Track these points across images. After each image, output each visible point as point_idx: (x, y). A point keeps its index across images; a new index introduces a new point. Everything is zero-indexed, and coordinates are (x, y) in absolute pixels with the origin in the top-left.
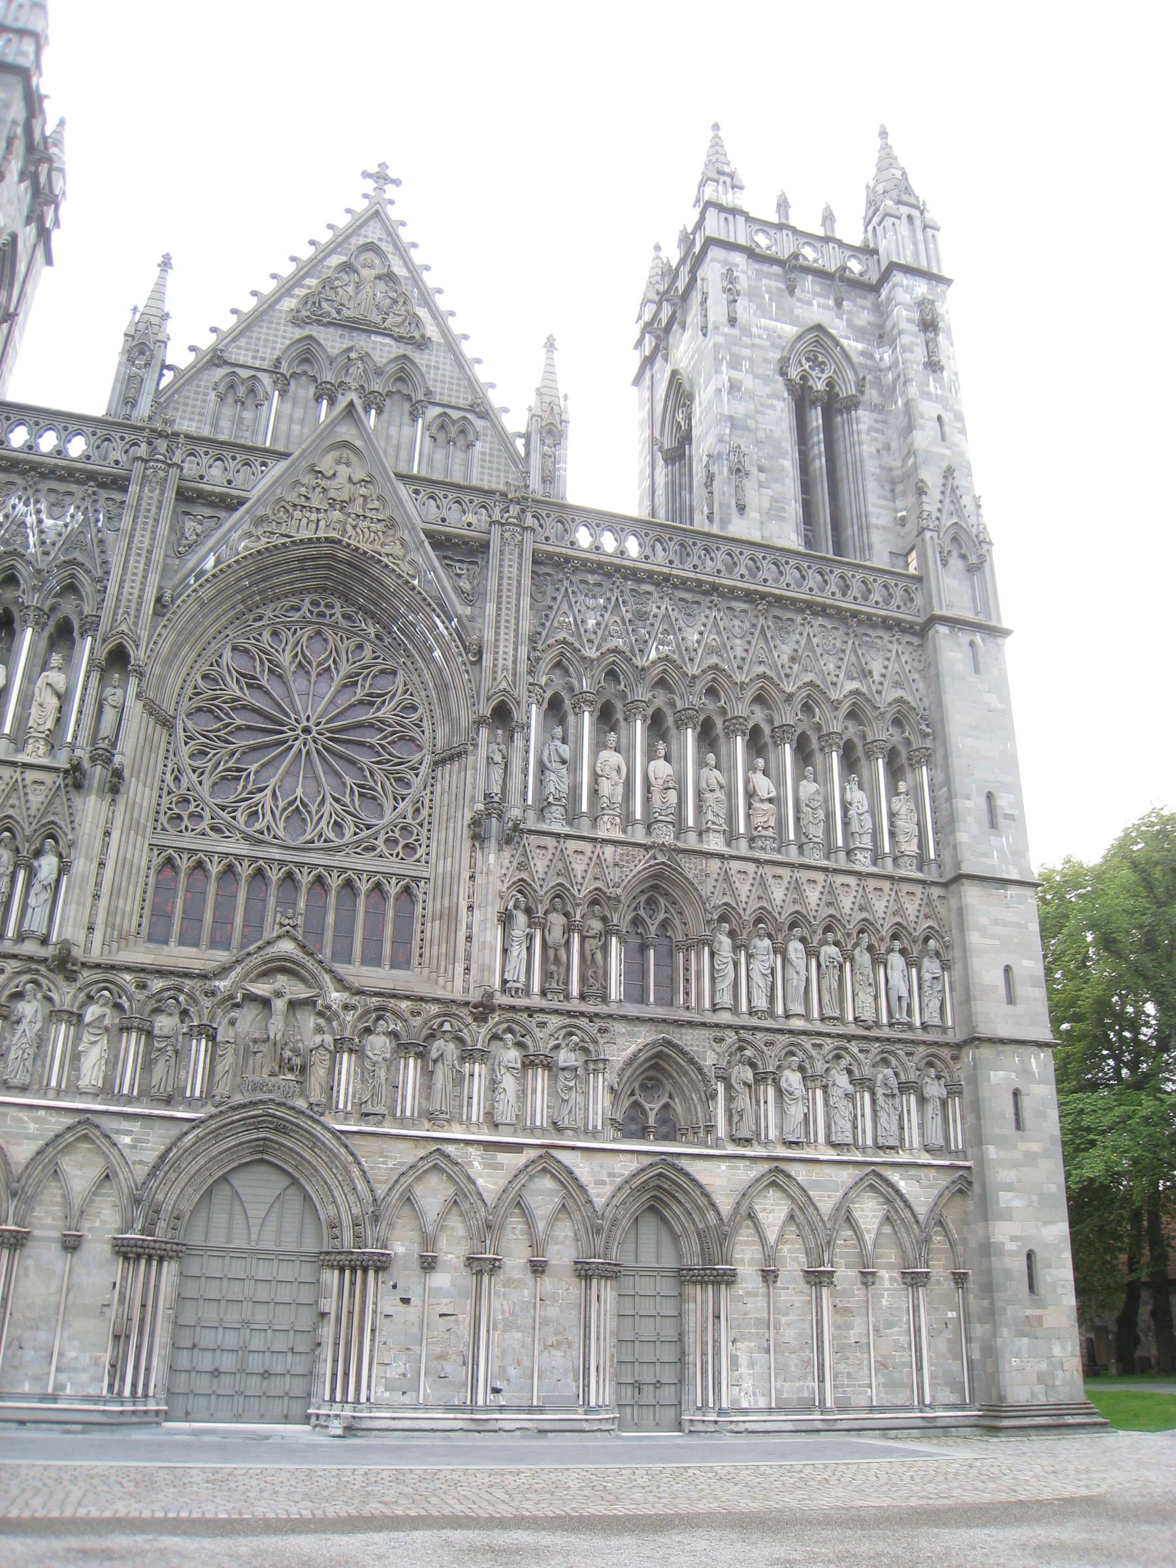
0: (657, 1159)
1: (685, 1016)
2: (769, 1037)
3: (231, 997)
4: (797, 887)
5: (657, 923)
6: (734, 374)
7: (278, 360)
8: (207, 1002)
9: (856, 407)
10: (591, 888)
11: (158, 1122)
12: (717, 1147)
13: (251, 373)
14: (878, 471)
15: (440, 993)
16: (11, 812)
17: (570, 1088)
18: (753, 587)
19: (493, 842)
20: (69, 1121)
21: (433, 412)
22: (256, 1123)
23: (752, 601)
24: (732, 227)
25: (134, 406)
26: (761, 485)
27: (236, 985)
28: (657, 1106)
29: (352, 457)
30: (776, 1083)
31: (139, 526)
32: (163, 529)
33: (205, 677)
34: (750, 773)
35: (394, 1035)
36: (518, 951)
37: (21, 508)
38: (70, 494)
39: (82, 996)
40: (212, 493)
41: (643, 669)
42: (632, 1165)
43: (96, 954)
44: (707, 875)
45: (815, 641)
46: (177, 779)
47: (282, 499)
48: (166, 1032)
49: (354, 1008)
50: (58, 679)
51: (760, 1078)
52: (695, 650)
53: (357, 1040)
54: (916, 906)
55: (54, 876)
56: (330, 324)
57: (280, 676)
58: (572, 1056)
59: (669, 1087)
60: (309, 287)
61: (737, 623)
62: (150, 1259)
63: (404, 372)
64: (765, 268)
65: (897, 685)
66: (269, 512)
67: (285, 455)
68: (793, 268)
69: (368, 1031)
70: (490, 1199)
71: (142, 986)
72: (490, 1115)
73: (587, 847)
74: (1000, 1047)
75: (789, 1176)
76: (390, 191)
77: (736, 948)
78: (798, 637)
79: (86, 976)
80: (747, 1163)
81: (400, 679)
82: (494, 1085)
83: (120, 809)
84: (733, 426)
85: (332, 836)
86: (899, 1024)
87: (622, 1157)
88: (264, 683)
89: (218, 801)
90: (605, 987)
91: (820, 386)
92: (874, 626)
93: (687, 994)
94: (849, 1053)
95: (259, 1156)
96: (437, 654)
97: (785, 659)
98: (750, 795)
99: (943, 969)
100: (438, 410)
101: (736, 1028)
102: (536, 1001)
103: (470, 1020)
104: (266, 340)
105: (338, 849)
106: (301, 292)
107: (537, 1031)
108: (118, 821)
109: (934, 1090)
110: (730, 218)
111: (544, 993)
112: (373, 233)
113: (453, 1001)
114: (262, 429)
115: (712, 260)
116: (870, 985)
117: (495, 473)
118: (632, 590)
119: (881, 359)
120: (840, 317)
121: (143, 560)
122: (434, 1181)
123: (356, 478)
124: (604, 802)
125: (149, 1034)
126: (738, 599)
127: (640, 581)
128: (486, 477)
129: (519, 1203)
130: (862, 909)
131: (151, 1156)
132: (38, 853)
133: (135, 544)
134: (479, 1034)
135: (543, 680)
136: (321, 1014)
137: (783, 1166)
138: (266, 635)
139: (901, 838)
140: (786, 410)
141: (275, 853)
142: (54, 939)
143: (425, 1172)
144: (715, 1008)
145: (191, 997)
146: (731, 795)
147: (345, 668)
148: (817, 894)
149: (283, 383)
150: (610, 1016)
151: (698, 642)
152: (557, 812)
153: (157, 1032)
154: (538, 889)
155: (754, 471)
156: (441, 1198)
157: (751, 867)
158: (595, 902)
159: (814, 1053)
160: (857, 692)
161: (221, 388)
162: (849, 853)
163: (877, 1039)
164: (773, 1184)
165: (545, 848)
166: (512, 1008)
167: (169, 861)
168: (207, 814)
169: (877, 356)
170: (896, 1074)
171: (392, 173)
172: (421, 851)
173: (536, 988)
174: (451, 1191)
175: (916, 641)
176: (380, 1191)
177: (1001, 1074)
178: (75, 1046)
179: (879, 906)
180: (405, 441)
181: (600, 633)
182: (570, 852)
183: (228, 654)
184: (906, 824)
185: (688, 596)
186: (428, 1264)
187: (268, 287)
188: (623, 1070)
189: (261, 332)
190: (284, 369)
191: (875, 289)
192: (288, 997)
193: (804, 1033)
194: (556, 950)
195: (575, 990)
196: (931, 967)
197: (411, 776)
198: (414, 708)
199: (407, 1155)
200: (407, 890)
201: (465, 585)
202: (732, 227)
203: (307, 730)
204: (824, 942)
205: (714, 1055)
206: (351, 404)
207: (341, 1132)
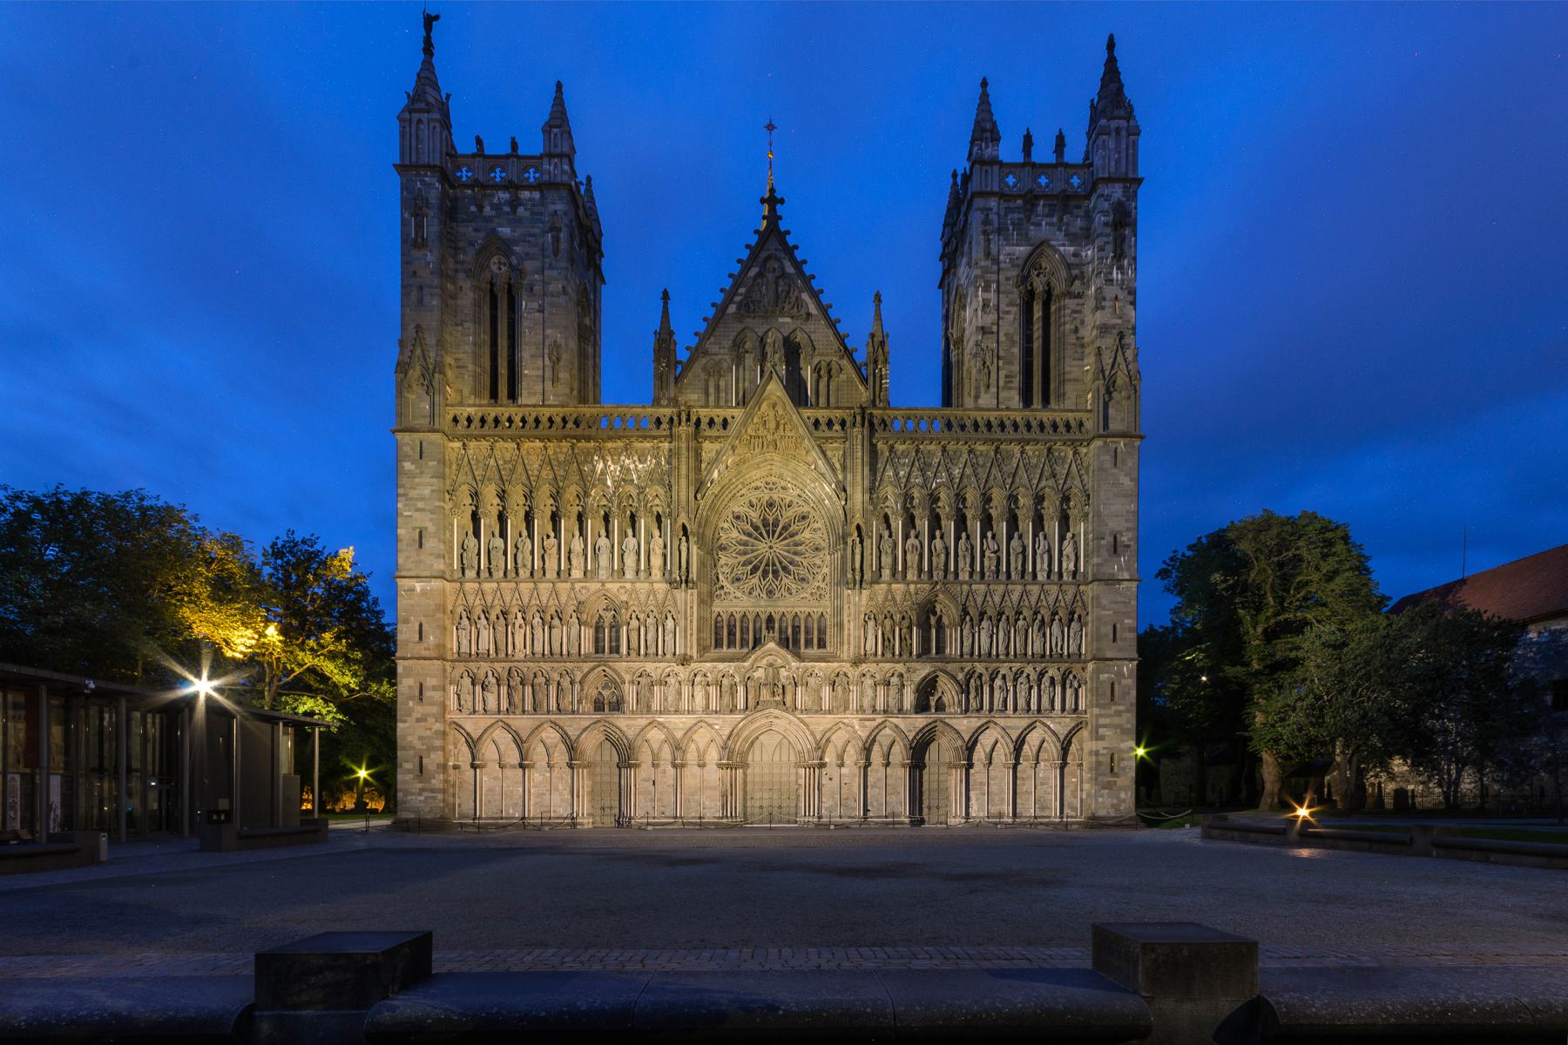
6: (987, 295)
14: (1074, 341)
24: (990, 178)
36: (871, 637)
37: (627, 461)
60: (741, 295)
64: (1011, 205)
68: (1031, 199)
84: (984, 333)
93: (951, 648)
96: (827, 502)
106: (737, 299)
110: (989, 169)
111: (883, 655)
115: (977, 209)
119: (1086, 256)
120: (1060, 229)
124: (909, 564)
131: (727, 732)
142: (677, 653)
173: (880, 652)
176: (818, 737)
177: (1106, 675)
186: (841, 765)
188: (919, 684)
191: (1088, 197)
195: (897, 653)
202: (990, 178)
203: (771, 548)
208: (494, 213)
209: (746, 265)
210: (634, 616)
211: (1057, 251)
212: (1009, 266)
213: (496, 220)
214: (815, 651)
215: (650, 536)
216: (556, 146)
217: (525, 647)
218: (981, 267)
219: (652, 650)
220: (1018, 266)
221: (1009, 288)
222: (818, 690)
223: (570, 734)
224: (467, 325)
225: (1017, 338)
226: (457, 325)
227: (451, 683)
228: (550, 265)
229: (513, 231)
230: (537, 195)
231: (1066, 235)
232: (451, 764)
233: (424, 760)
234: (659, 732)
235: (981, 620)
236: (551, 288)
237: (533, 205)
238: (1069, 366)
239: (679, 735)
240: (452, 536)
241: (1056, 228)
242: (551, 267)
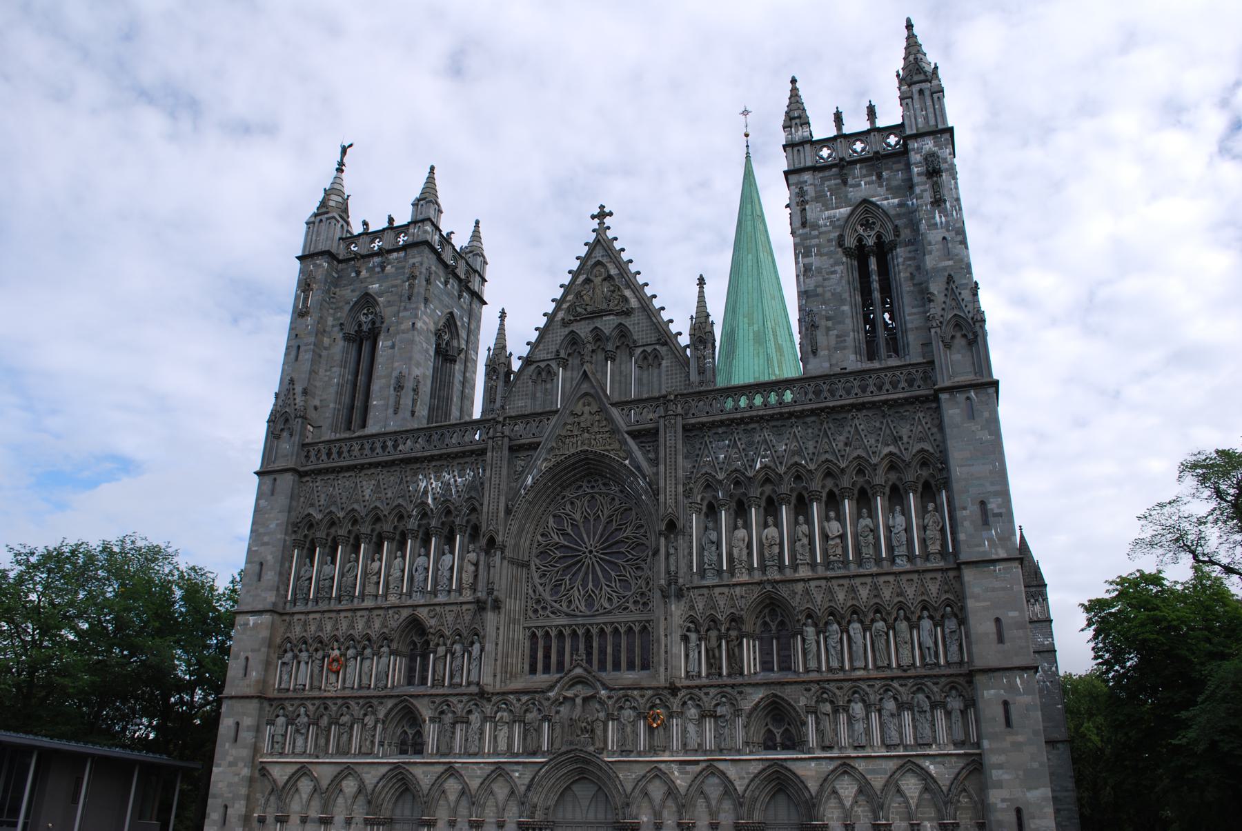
0: (772, 763)
1: (790, 677)
2: (839, 684)
3: (557, 700)
4: (853, 589)
5: (776, 622)
6: (807, 260)
7: (558, 351)
8: (546, 704)
9: (895, 248)
10: (728, 613)
11: (529, 765)
12: (809, 753)
13: (545, 363)
14: (912, 288)
15: (654, 684)
16: (458, 627)
17: (724, 727)
18: (814, 406)
19: (673, 598)
20: (492, 768)
21: (639, 351)
22: (577, 759)
23: (818, 415)
24: (802, 155)
25: (494, 402)
26: (828, 329)
27: (559, 694)
28: (781, 731)
29: (591, 399)
30: (846, 709)
31: (493, 473)
32: (504, 471)
33: (542, 535)
34: (826, 524)
35: (634, 708)
36: (694, 655)
38: (467, 463)
39: (495, 708)
40: (524, 444)
41: (750, 478)
42: (760, 766)
43: (499, 687)
44: (796, 593)
45: (860, 428)
46: (534, 591)
47: (559, 435)
48: (530, 721)
49: (613, 697)
50: (472, 556)
51: (836, 711)
52: (783, 456)
53: (616, 713)
54: (937, 587)
55: (479, 653)
56: (581, 319)
57: (577, 526)
58: (724, 708)
59: (787, 719)
60: (570, 301)
61: (810, 431)
63: (623, 332)
64: (827, 173)
65: (921, 440)
66: (555, 445)
67: (557, 411)
69: (621, 708)
70: (683, 791)
71: (519, 700)
72: (685, 745)
73: (726, 590)
74: (991, 674)
75: (853, 767)
76: (608, 221)
77: (818, 634)
78: (849, 428)
79: (494, 699)
80: (828, 761)
81: (633, 512)
82: (685, 731)
83: (502, 616)
84: (807, 297)
85: (606, 605)
86: (927, 664)
87: (753, 763)
88: (569, 531)
89: (553, 599)
90: (742, 668)
91: (870, 242)
92: (902, 405)
94: (893, 688)
95: (581, 776)
97: (841, 445)
98: (825, 537)
99: (960, 625)
100: (641, 349)
101: (818, 682)
102: (704, 681)
103: (669, 696)
104: (552, 341)
105: (610, 612)
106: (565, 306)
107: (705, 698)
108: (502, 622)
109: (955, 704)
110: (801, 148)
111: (708, 676)
112: (598, 254)
113: (658, 688)
114: (555, 392)
116: (906, 643)
117: (674, 377)
118: (744, 430)
119: (913, 204)
120: (881, 186)
121: (497, 490)
122: (657, 782)
123: (593, 411)
125: (524, 721)
126: (808, 416)
127: (748, 423)
128: (670, 381)
129: (702, 792)
130: (898, 595)
131: (527, 781)
132: (472, 643)
133: (493, 483)
134: (675, 704)
135: (699, 497)
136: (599, 702)
137: (847, 761)
138: (568, 506)
139: (929, 543)
140: (845, 271)
141: (580, 621)
143: (653, 777)
144: (807, 671)
145: (539, 701)
146: (811, 537)
147: (606, 513)
148: (867, 591)
149: (564, 364)
150: (742, 684)
151: (785, 450)
152: (709, 574)
153: (526, 721)
154: (699, 619)
155: (823, 323)
156: (662, 792)
157: (823, 583)
158: (733, 620)
159: (868, 689)
160: (891, 454)
161: (534, 377)
162: (892, 559)
163: (910, 677)
164: (845, 772)
165: (703, 595)
166: (688, 687)
167: (534, 635)
168: (549, 607)
169: (910, 203)
170: (928, 697)
171: (607, 210)
172: (651, 605)
174: (666, 788)
175: (934, 405)
176: (629, 791)
178: (495, 731)
179: (910, 591)
180: (628, 372)
181: (726, 462)
182: (716, 594)
183: (551, 520)
184: (933, 533)
185: (779, 423)
187: (550, 307)
189: (549, 337)
190: (562, 355)
192: (581, 697)
193: (860, 679)
194: (713, 651)
196: (951, 624)
197: (643, 565)
198: (642, 526)
199: (640, 771)
200: (645, 628)
201: (652, 456)
203: (591, 552)
204: (873, 621)
205: (805, 699)
206: (585, 371)
207: (610, 762)
208: (368, 275)
209: (575, 274)
210: (441, 643)
211: (878, 207)
212: (831, 228)
213: (369, 280)
214: (629, 677)
215: (465, 550)
216: (421, 214)
217: (337, 682)
218: (800, 235)
219: (457, 680)
220: (839, 226)
221: (832, 248)
222: (634, 724)
223: (367, 782)
224: (334, 369)
225: (846, 295)
226: (326, 371)
227: (267, 724)
228: (405, 307)
229: (380, 286)
230: (402, 254)
231: (887, 190)
232: (255, 815)
233: (230, 811)
234: (456, 781)
235: (827, 623)
236: (403, 327)
237: (398, 262)
238: (909, 315)
239: (474, 784)
240: (290, 568)
241: (877, 185)
242: (405, 309)
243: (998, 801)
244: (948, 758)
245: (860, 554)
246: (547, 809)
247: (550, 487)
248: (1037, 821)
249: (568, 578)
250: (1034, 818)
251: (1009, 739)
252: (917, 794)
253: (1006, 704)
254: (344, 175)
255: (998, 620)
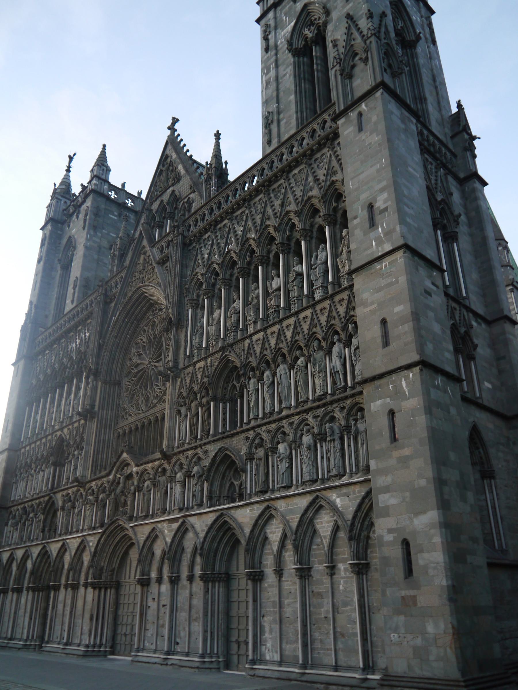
27: (115, 476)
62: (100, 589)
74: (377, 383)
203: (150, 362)
243: (385, 533)
244: (352, 487)
245: (289, 297)
246: (113, 570)
247: (128, 322)
248: (425, 555)
249: (138, 387)
250: (422, 551)
251: (396, 454)
252: (329, 533)
253: (392, 413)
254: (70, 174)
255: (384, 322)
